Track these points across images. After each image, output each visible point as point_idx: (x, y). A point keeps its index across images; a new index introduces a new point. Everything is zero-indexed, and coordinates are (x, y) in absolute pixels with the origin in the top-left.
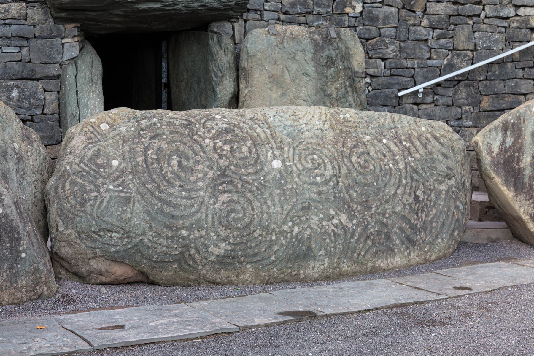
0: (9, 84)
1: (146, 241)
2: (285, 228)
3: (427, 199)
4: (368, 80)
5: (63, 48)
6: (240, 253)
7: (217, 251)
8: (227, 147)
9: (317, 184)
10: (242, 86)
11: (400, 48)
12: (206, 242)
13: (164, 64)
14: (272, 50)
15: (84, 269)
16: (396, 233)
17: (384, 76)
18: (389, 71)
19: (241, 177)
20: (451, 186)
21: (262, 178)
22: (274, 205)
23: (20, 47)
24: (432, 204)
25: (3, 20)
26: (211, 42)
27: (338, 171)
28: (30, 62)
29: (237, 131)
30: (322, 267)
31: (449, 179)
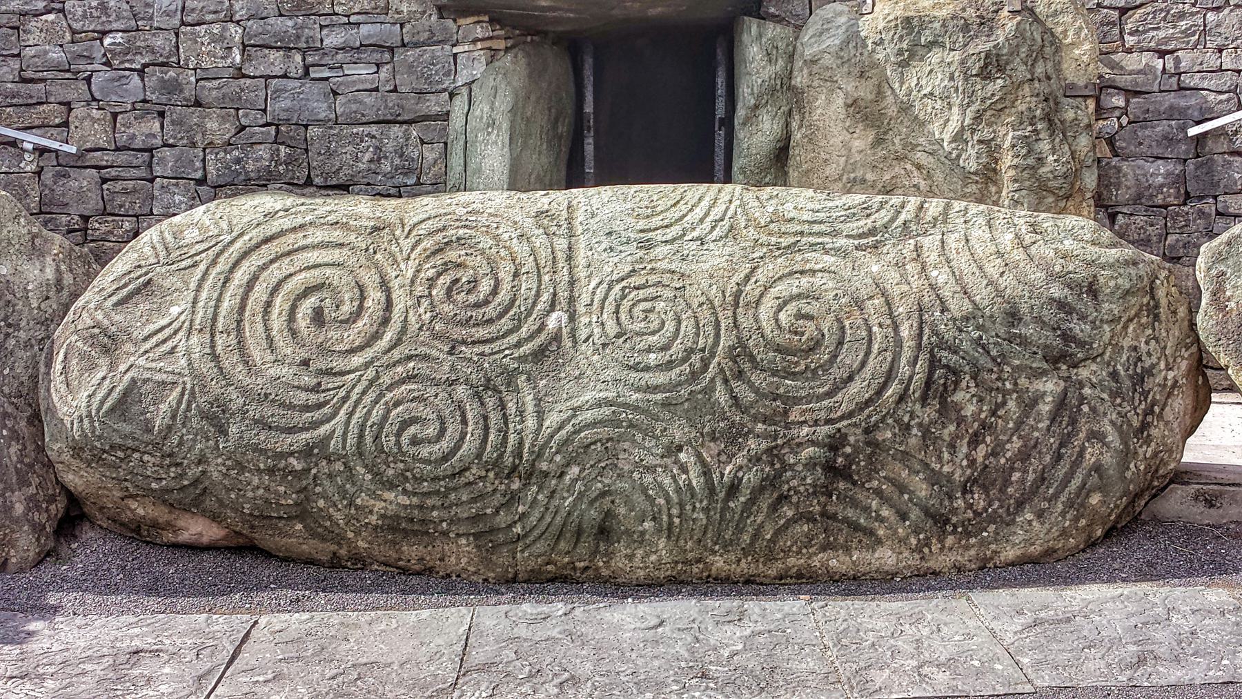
0: (355, 131)
1: (215, 474)
2: (544, 466)
3: (993, 413)
4: (1119, 101)
5: (455, 64)
6: (435, 514)
7: (379, 506)
8: (445, 280)
9: (647, 369)
10: (795, 125)
11: (1205, 25)
12: (348, 486)
13: (721, 81)
14: (856, 47)
15: (126, 516)
16: (878, 493)
17: (1161, 91)
18: (1174, 79)
19: (453, 348)
20: (1081, 385)
21: (507, 352)
22: (521, 413)
23: (378, 65)
24: (1011, 425)
25: (348, 16)
26: (745, 37)
27: (710, 341)
28: (395, 90)
29: (486, 243)
30: (653, 558)
31: (1075, 366)
